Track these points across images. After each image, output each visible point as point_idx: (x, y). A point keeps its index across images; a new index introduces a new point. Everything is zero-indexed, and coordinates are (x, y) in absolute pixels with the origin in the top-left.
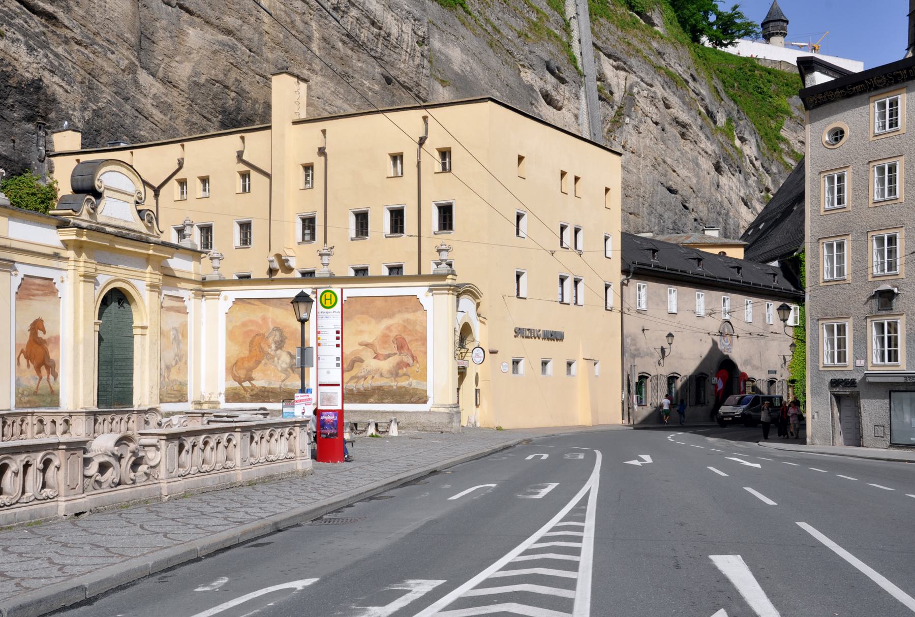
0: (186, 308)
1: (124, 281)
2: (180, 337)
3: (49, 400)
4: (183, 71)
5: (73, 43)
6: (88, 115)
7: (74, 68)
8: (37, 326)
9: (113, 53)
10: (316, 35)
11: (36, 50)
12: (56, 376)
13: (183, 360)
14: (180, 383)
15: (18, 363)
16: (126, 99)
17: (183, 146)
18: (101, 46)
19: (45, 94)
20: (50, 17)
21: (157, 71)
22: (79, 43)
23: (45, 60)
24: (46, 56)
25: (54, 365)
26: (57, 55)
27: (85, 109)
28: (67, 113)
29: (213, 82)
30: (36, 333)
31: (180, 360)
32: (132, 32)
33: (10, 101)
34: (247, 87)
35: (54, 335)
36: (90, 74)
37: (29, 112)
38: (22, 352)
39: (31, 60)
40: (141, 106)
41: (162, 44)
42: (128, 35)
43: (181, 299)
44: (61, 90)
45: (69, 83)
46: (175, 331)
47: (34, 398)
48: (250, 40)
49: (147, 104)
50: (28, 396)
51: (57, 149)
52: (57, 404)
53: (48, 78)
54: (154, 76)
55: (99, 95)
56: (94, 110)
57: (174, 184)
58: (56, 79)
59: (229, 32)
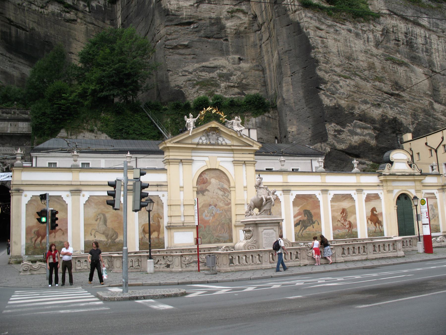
0: (436, 197)
1: (405, 190)
2: (434, 208)
3: (380, 234)
5: (407, 102)
6: (415, 126)
7: (408, 110)
8: (373, 210)
9: (422, 100)
11: (393, 108)
12: (382, 226)
13: (437, 216)
14: (436, 225)
15: (368, 223)
16: (430, 116)
17: (443, 132)
18: (418, 99)
19: (398, 122)
20: (398, 95)
21: (442, 101)
22: (409, 101)
23: (397, 111)
24: (397, 109)
25: (381, 222)
26: (401, 108)
27: (414, 124)
28: (407, 127)
30: (373, 212)
31: (435, 216)
32: (429, 91)
33: (387, 128)
35: (380, 212)
36: (414, 110)
37: (393, 130)
38: (369, 219)
39: (392, 112)
40: (436, 116)
42: (428, 92)
43: (433, 194)
44: (404, 120)
45: (406, 116)
46: (431, 206)
47: (375, 234)
49: (439, 115)
50: (372, 233)
52: (384, 236)
53: (398, 116)
55: (418, 117)
56: (417, 123)
57: (441, 147)
58: (402, 116)
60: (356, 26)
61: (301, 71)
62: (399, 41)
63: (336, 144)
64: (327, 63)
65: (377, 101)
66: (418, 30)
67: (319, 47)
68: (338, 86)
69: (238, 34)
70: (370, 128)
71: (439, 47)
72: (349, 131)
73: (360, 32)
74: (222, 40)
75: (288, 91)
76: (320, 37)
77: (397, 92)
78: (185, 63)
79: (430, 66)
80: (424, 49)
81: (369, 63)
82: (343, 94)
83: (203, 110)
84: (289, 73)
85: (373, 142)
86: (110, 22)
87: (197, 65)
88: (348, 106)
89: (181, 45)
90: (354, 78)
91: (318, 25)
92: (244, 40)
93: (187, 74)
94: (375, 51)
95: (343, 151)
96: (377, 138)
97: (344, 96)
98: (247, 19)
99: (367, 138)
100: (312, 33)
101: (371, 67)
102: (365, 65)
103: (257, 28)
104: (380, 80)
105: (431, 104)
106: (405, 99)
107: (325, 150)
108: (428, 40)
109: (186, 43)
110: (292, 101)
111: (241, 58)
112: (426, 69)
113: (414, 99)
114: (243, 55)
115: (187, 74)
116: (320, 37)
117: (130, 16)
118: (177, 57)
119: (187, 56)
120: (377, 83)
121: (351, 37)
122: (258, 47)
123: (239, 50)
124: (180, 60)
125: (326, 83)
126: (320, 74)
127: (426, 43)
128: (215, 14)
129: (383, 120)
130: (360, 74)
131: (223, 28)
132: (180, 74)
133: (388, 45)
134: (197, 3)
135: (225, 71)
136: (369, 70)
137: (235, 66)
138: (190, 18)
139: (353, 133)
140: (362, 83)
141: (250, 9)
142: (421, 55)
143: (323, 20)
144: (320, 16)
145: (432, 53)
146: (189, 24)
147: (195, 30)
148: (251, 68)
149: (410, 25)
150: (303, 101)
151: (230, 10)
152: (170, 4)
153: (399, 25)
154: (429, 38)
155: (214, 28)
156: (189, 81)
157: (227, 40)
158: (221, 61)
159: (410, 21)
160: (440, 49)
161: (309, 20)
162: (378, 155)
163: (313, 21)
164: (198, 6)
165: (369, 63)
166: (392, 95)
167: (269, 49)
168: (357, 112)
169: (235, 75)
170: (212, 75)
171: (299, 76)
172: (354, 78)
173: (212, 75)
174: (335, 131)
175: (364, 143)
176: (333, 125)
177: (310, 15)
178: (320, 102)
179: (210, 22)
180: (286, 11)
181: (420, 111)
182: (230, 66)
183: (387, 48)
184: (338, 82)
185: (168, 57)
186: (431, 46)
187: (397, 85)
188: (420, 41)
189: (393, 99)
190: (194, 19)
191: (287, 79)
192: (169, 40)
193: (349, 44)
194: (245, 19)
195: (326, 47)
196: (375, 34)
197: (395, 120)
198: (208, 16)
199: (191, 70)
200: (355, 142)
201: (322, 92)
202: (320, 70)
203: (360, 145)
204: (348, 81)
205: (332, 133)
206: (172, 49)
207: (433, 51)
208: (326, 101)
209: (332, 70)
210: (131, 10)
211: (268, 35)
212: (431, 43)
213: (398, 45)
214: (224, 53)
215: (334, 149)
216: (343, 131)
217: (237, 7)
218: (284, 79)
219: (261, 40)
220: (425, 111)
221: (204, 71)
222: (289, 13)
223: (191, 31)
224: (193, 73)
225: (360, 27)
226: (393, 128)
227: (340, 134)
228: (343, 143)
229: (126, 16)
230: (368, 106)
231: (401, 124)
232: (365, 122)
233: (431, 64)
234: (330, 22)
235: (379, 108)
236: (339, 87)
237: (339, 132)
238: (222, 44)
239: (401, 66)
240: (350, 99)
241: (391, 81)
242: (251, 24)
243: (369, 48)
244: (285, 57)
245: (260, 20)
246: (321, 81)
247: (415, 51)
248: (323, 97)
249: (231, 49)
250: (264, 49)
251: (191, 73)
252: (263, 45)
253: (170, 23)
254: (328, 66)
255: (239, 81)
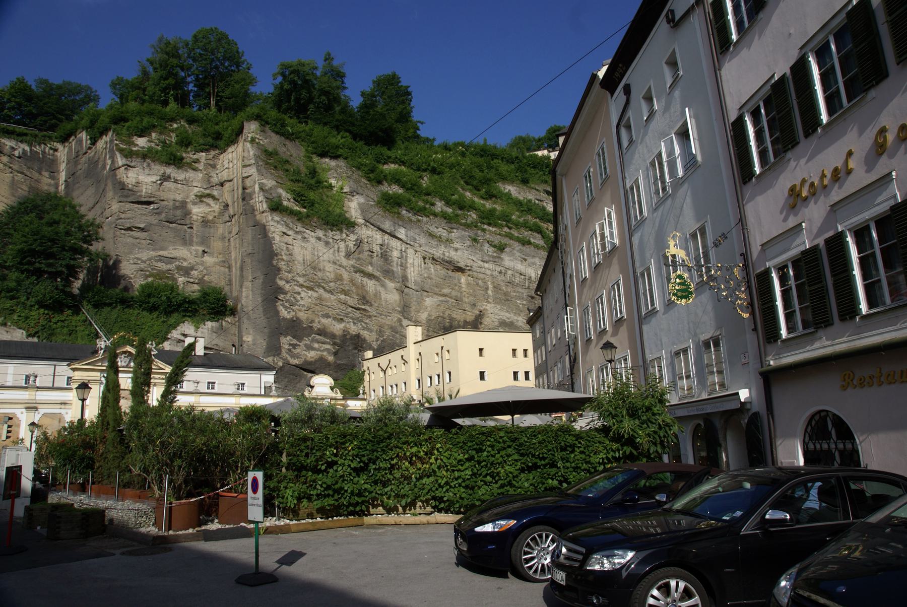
4: (423, 316)
10: (490, 286)
16: (397, 333)
20: (364, 310)
26: (366, 323)
29: (437, 318)
34: (455, 316)
41: (414, 308)
48: (456, 296)
51: (366, 358)
53: (362, 332)
54: (410, 320)
58: (365, 332)
59: (445, 296)
60: (327, 234)
61: (262, 277)
62: (373, 252)
63: (289, 358)
64: (289, 272)
65: (340, 315)
66: (394, 243)
67: (283, 254)
68: (298, 297)
69: (205, 222)
70: (329, 344)
71: (415, 261)
72: (306, 345)
73: (331, 241)
74: (185, 227)
75: (247, 297)
76: (287, 244)
77: (363, 307)
78: (139, 248)
79: (403, 281)
80: (399, 263)
81: (336, 274)
82: (304, 306)
83: (116, 334)
84: (250, 278)
85: (331, 358)
86: (50, 175)
87: (153, 253)
88: (308, 319)
89: (136, 228)
90: (317, 289)
91: (285, 231)
92: (212, 230)
93: (139, 262)
94: (344, 262)
95: (296, 366)
96: (335, 354)
97: (303, 309)
98: (217, 206)
99: (325, 353)
100: (277, 238)
101: (339, 278)
102: (332, 276)
103: (228, 219)
104: (346, 293)
105: (400, 321)
106: (371, 314)
107: (277, 363)
108: (404, 253)
109: (142, 226)
110: (250, 308)
111: (206, 250)
112: (398, 285)
113: (381, 315)
114: (209, 247)
115: (139, 262)
116: (287, 244)
117: (77, 174)
118: (130, 240)
119: (142, 241)
120: (343, 297)
121: (321, 246)
122: (227, 241)
123: (204, 241)
124: (133, 244)
125: (286, 293)
126: (281, 283)
127: (402, 257)
128: (181, 196)
129: (345, 336)
130: (325, 286)
131: (188, 213)
132: (131, 262)
133: (361, 256)
134: (160, 180)
135: (185, 264)
136: (335, 282)
137: (197, 259)
138: (150, 197)
139: (309, 348)
140: (327, 295)
141: (222, 196)
142: (395, 269)
143: (291, 225)
144: (289, 221)
145: (407, 268)
146: (149, 203)
147: (155, 211)
148: (215, 264)
149: (387, 237)
150: (261, 309)
151: (199, 194)
152: (127, 177)
153: (375, 236)
154: (405, 252)
155: (179, 213)
156: (141, 271)
157: (192, 228)
158: (182, 252)
159: (387, 233)
160: (416, 264)
161: (275, 224)
162: (336, 372)
163: (279, 226)
164: (161, 184)
165: (336, 274)
166: (358, 309)
167: (238, 245)
168: (316, 326)
169: (196, 270)
170: (169, 267)
171: (259, 281)
172: (317, 289)
173: (169, 267)
174: (290, 345)
175: (321, 359)
176: (289, 338)
177: (277, 218)
178: (277, 312)
179: (174, 204)
180: (254, 210)
181: (386, 327)
182: (192, 260)
183: (359, 259)
184: (299, 293)
185: (119, 239)
186: (406, 260)
187: (364, 299)
188: (396, 254)
189: (358, 314)
190: (154, 199)
191: (247, 284)
192: (121, 219)
193: (316, 253)
194: (216, 207)
195: (291, 255)
196: (347, 243)
197: (358, 336)
198: (172, 197)
199: (144, 259)
200: (311, 357)
201: (281, 303)
202: (281, 279)
203: (316, 361)
204: (310, 292)
205: (287, 347)
206: (124, 230)
207: (408, 265)
208: (284, 313)
209: (294, 280)
210: (79, 167)
211: (238, 229)
212: (406, 257)
213: (372, 257)
214: (186, 242)
215: (287, 363)
216: (299, 345)
217: (208, 192)
218: (245, 283)
219: (230, 232)
220: (393, 329)
221: (160, 260)
222: (256, 213)
223: (149, 212)
224: (147, 262)
225: (331, 236)
226: (355, 344)
227: (295, 348)
228: (298, 357)
229: (72, 173)
230: (330, 320)
231: (364, 340)
232: (325, 336)
233: (405, 279)
234: (300, 228)
235: (341, 323)
236: (299, 299)
237: (294, 346)
238: (185, 231)
239: (371, 279)
240: (310, 312)
241: (358, 295)
242: (221, 213)
243: (338, 258)
244: (248, 260)
245: (231, 211)
246: (280, 290)
247: (389, 264)
248: (281, 308)
249: (195, 239)
250: (232, 244)
251: (145, 262)
252: (232, 239)
253: (125, 199)
254: (290, 275)
255: (200, 276)
